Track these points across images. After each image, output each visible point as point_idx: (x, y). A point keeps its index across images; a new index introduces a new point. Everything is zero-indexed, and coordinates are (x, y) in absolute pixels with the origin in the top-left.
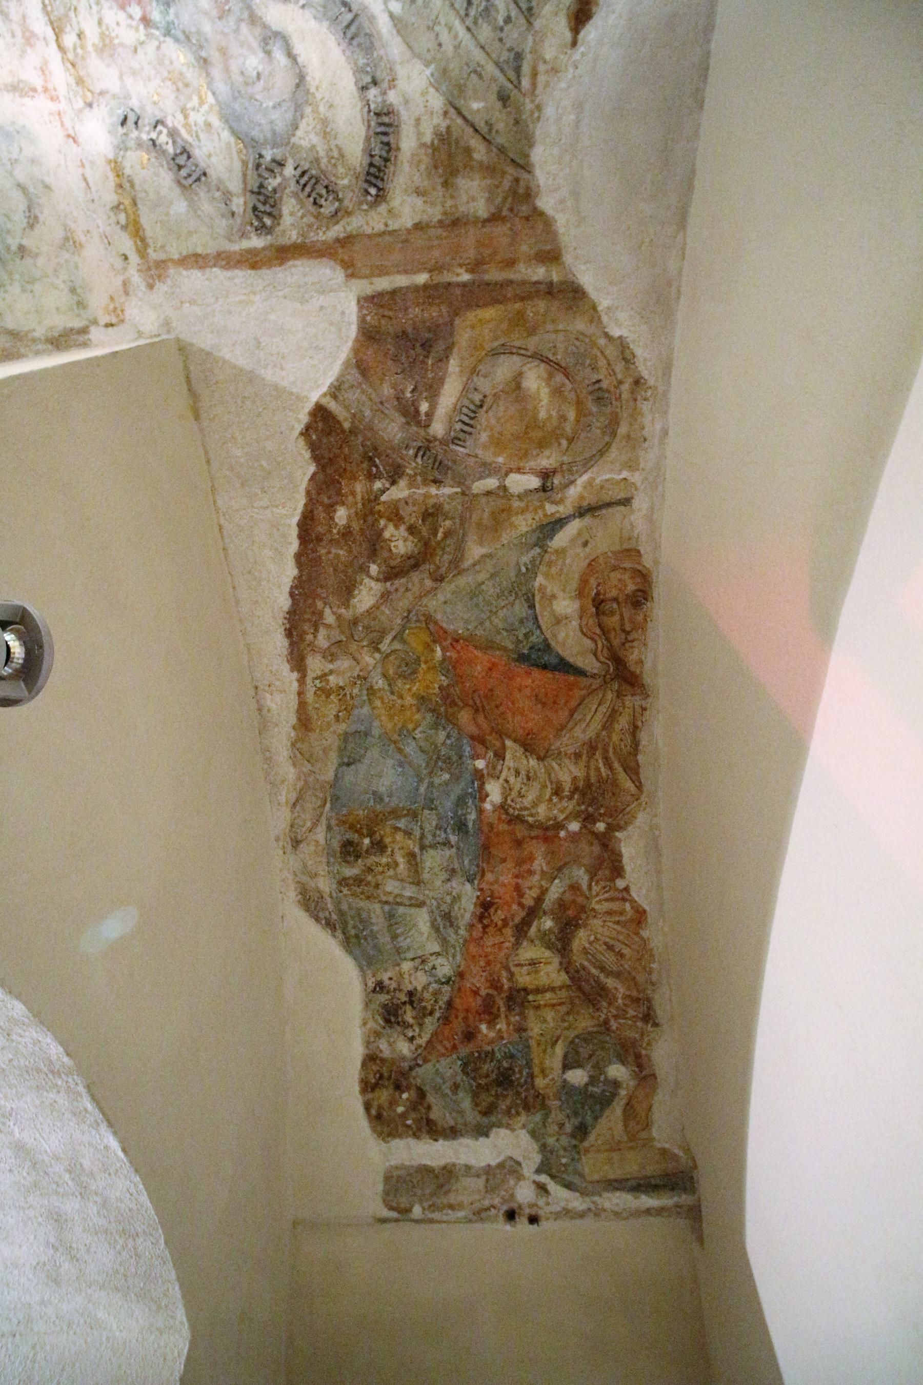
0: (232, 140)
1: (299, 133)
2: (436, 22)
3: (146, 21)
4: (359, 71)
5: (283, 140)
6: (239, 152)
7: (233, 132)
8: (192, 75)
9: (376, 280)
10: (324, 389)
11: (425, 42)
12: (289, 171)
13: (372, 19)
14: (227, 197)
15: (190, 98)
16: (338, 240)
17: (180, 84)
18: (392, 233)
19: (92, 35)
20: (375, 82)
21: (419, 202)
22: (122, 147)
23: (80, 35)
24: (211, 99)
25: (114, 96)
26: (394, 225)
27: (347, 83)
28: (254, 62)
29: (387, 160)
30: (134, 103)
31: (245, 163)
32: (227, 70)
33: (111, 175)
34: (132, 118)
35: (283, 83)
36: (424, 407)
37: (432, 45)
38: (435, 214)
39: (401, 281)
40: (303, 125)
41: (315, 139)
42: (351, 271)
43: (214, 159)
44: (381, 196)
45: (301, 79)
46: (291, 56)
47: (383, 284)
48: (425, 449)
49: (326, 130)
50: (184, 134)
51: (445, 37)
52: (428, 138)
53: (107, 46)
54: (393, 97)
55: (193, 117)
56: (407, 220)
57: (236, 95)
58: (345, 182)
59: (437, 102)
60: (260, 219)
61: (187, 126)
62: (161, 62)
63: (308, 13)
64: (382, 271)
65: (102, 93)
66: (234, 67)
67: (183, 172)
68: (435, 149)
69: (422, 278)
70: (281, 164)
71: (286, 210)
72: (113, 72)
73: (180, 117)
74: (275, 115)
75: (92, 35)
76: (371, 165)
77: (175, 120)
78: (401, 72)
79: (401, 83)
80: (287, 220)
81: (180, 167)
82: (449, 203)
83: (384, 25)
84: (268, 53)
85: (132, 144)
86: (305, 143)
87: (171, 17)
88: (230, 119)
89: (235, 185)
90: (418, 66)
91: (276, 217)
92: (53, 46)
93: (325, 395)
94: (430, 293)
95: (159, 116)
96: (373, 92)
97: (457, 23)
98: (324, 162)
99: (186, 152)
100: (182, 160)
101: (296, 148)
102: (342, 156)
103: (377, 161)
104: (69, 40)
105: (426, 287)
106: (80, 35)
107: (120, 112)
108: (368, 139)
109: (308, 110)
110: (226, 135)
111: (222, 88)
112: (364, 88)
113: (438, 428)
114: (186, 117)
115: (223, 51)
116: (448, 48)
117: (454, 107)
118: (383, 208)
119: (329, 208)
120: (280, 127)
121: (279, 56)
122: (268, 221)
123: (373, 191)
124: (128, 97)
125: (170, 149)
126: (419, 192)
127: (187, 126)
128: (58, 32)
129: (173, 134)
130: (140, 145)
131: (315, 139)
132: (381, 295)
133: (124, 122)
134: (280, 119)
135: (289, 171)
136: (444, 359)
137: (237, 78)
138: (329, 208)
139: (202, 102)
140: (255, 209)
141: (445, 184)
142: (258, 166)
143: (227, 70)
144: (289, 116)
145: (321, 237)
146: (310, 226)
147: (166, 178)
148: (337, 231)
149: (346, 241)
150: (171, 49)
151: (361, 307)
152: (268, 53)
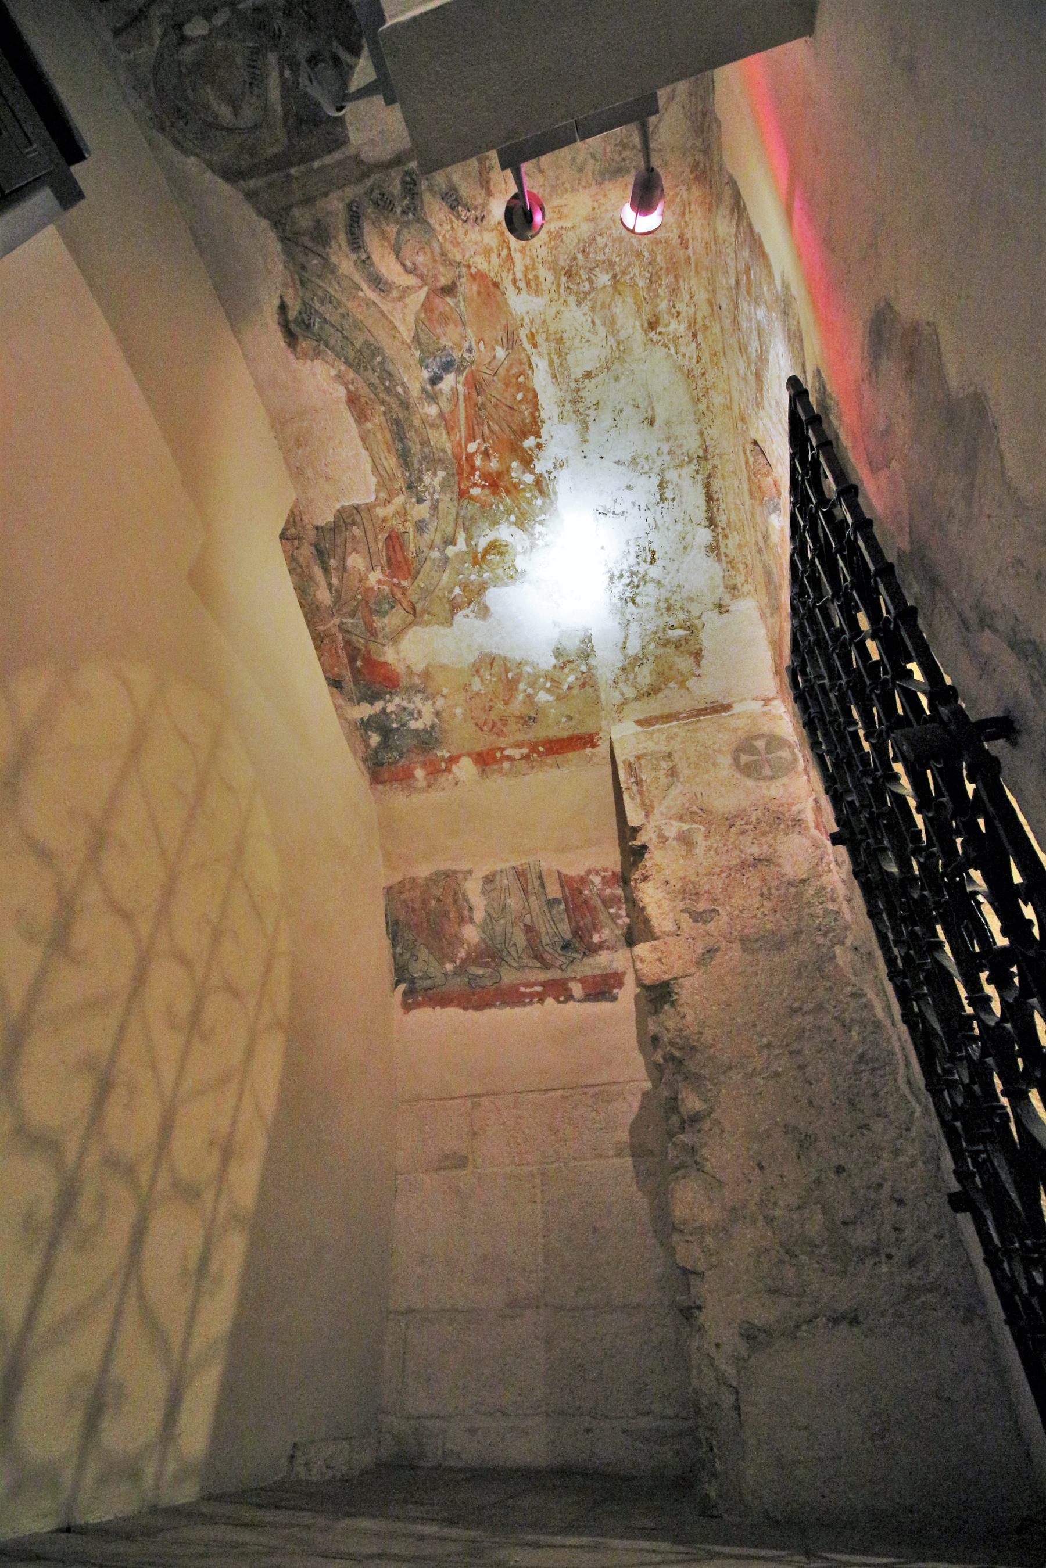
0: (429, 220)
1: (396, 230)
2: (342, 292)
3: (469, 267)
4: (372, 265)
5: (407, 224)
6: (425, 214)
7: (429, 224)
8: (448, 247)
9: (342, 157)
10: (357, 70)
11: (344, 284)
12: (399, 211)
13: (370, 287)
14: (430, 188)
15: (450, 236)
16: (368, 176)
17: (456, 243)
18: (340, 188)
19: (494, 258)
20: (363, 261)
21: (329, 209)
22: (484, 205)
23: (499, 255)
24: (440, 238)
25: (487, 230)
26: (340, 192)
27: (376, 258)
28: (420, 259)
29: (351, 226)
30: (477, 228)
31: (422, 209)
32: (432, 252)
33: (492, 188)
34: (479, 221)
35: (406, 252)
36: (287, 73)
37: (342, 283)
38: (320, 203)
39: (328, 160)
40: (395, 235)
41: (388, 229)
42: (357, 159)
43: (438, 208)
44: (349, 206)
45: (398, 257)
46: (403, 265)
47: (337, 156)
48: (276, 36)
49: (384, 236)
50: (454, 219)
51: (337, 287)
52: (333, 243)
53: (487, 253)
54: (354, 257)
55: (449, 227)
56: (334, 195)
57: (428, 243)
58: (369, 210)
59: (334, 259)
60: (412, 179)
61: (452, 222)
62: (463, 250)
63: (398, 284)
64: (340, 163)
65: (492, 230)
66: (429, 255)
67: (454, 197)
68: (328, 237)
69: (316, 164)
70: (404, 212)
71: (399, 186)
72: (486, 241)
73: (455, 226)
74: (408, 236)
75: (494, 258)
76: (358, 222)
77: (457, 223)
78: (353, 269)
79: (351, 264)
80: (397, 183)
81: (456, 200)
82: (313, 212)
83: (364, 286)
84: (414, 264)
85: (480, 207)
86: (392, 225)
87: (457, 271)
88: (429, 229)
89: (427, 197)
90: (345, 273)
91: (404, 182)
92: (512, 248)
93: (356, 65)
94: (306, 157)
95: (465, 225)
96: (364, 256)
97: (333, 293)
98: (382, 218)
99: (452, 208)
100: (455, 203)
101: (397, 222)
102: (373, 224)
103: (355, 225)
104: (504, 253)
105: (313, 159)
106: (499, 255)
107: (485, 222)
108: (362, 235)
109: (393, 242)
110: (432, 221)
111: (435, 245)
112: (368, 257)
113: (272, 58)
114: (452, 227)
115: (435, 261)
116: (335, 283)
117: (325, 259)
118: (347, 201)
119: (376, 194)
120: (405, 231)
121: (408, 263)
122: (408, 179)
123: (354, 209)
124: (480, 231)
125: (460, 208)
126: (329, 213)
127: (452, 222)
128: (509, 255)
129: (458, 217)
130: (476, 208)
131: (388, 229)
132: (338, 148)
133: (483, 218)
134: (406, 235)
135: (399, 211)
136: (286, 114)
137: (427, 249)
138: (376, 194)
139: (444, 236)
140: (415, 185)
141: (318, 221)
142: (415, 209)
143: (432, 252)
144: (401, 237)
145: (377, 176)
146: (384, 181)
147: (464, 191)
148: (369, 182)
149: (365, 175)
150: (458, 257)
151: (347, 136)
152: (414, 264)
